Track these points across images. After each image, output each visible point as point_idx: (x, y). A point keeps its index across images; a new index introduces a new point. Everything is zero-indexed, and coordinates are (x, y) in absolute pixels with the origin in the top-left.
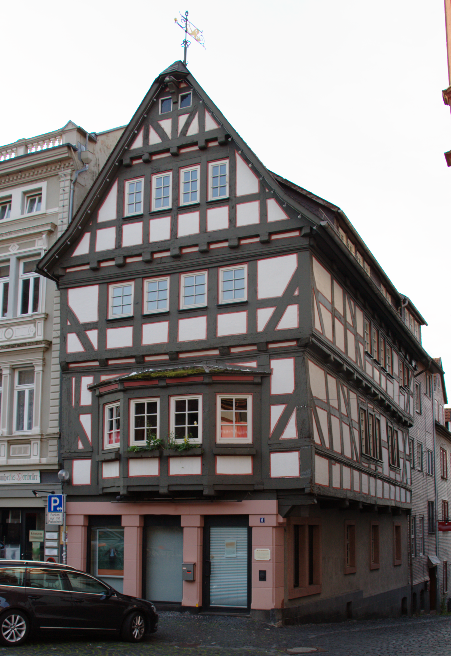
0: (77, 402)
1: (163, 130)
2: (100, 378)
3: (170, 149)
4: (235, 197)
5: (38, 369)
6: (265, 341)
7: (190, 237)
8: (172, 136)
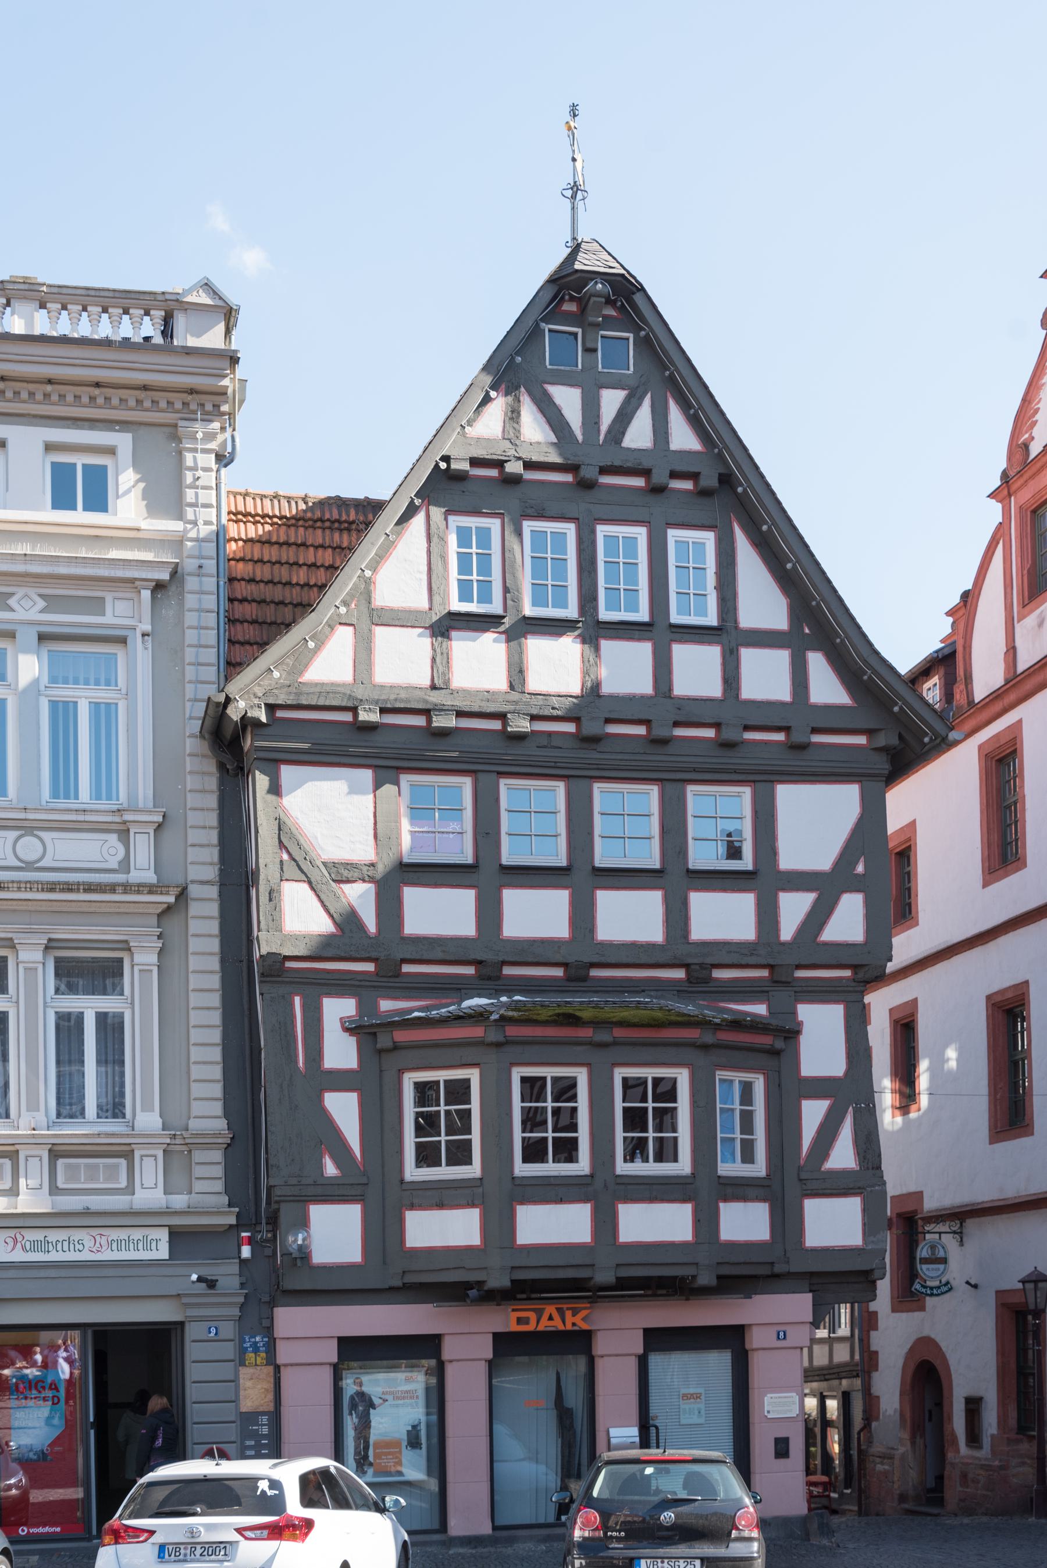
0: (314, 1060)
1: (558, 411)
2: (376, 1005)
3: (583, 466)
4: (737, 628)
6: (797, 963)
7: (631, 699)
8: (583, 434)
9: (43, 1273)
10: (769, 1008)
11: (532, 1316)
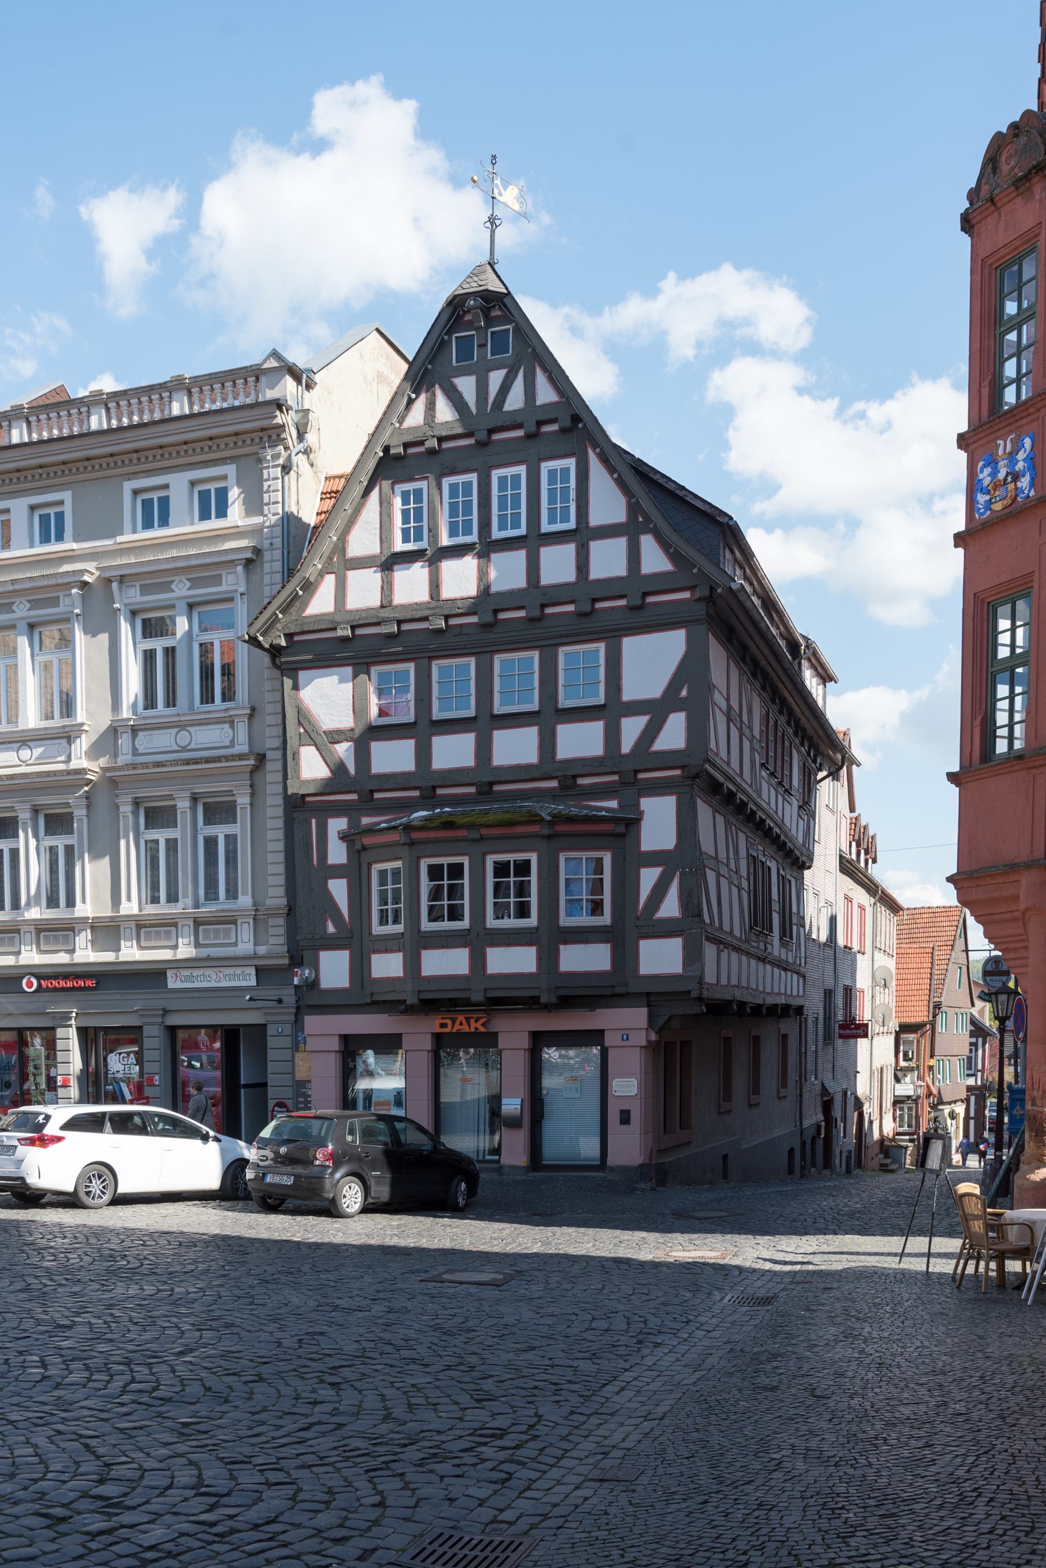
2: (360, 821)
4: (587, 527)
5: (243, 800)
9: (191, 995)
10: (619, 804)
11: (449, 1022)
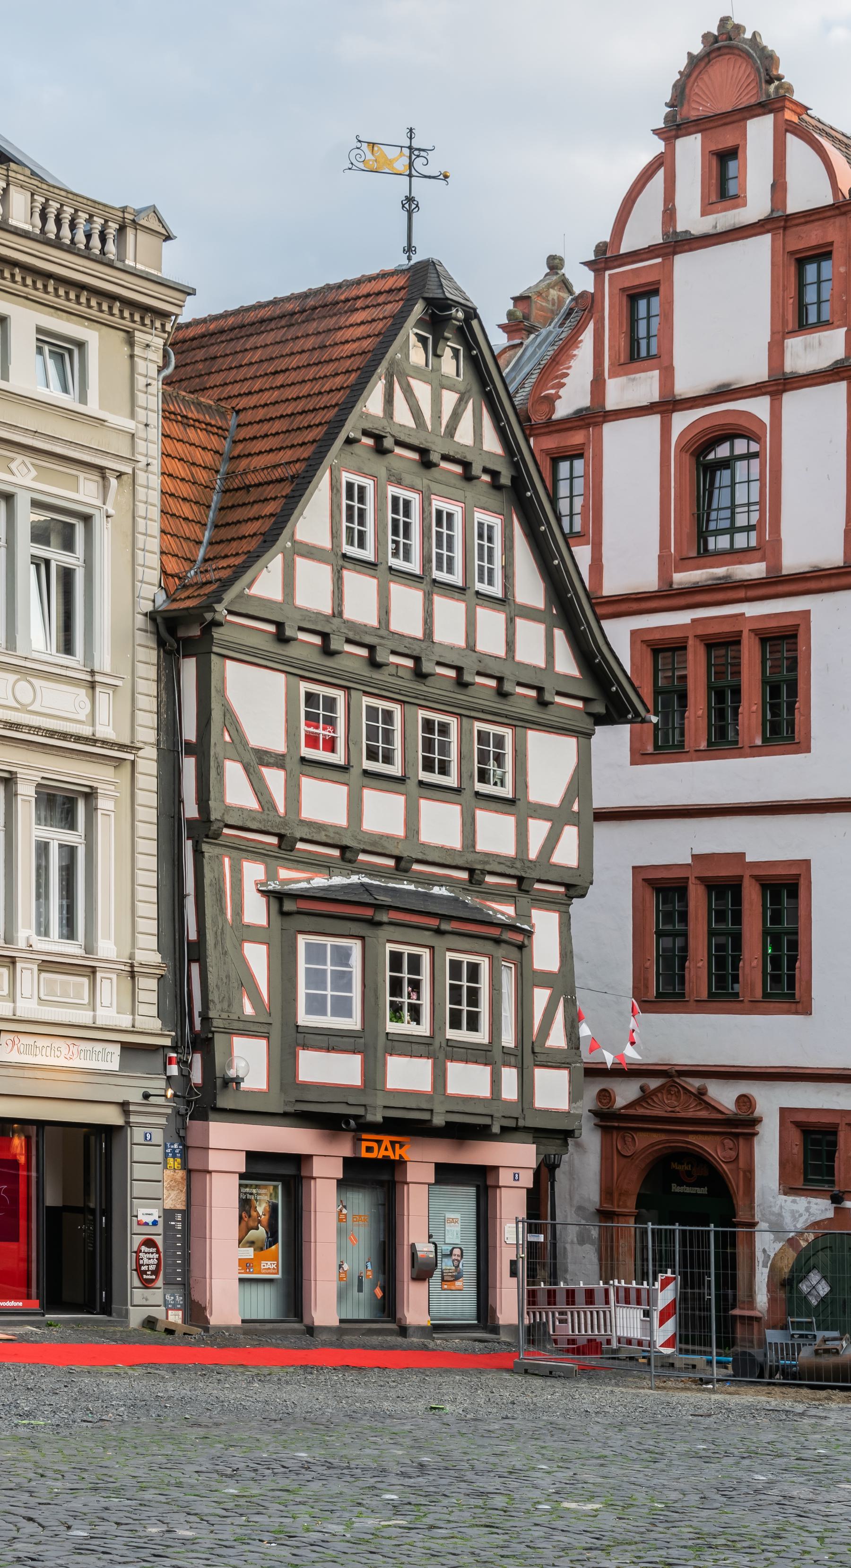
2: (277, 873)
